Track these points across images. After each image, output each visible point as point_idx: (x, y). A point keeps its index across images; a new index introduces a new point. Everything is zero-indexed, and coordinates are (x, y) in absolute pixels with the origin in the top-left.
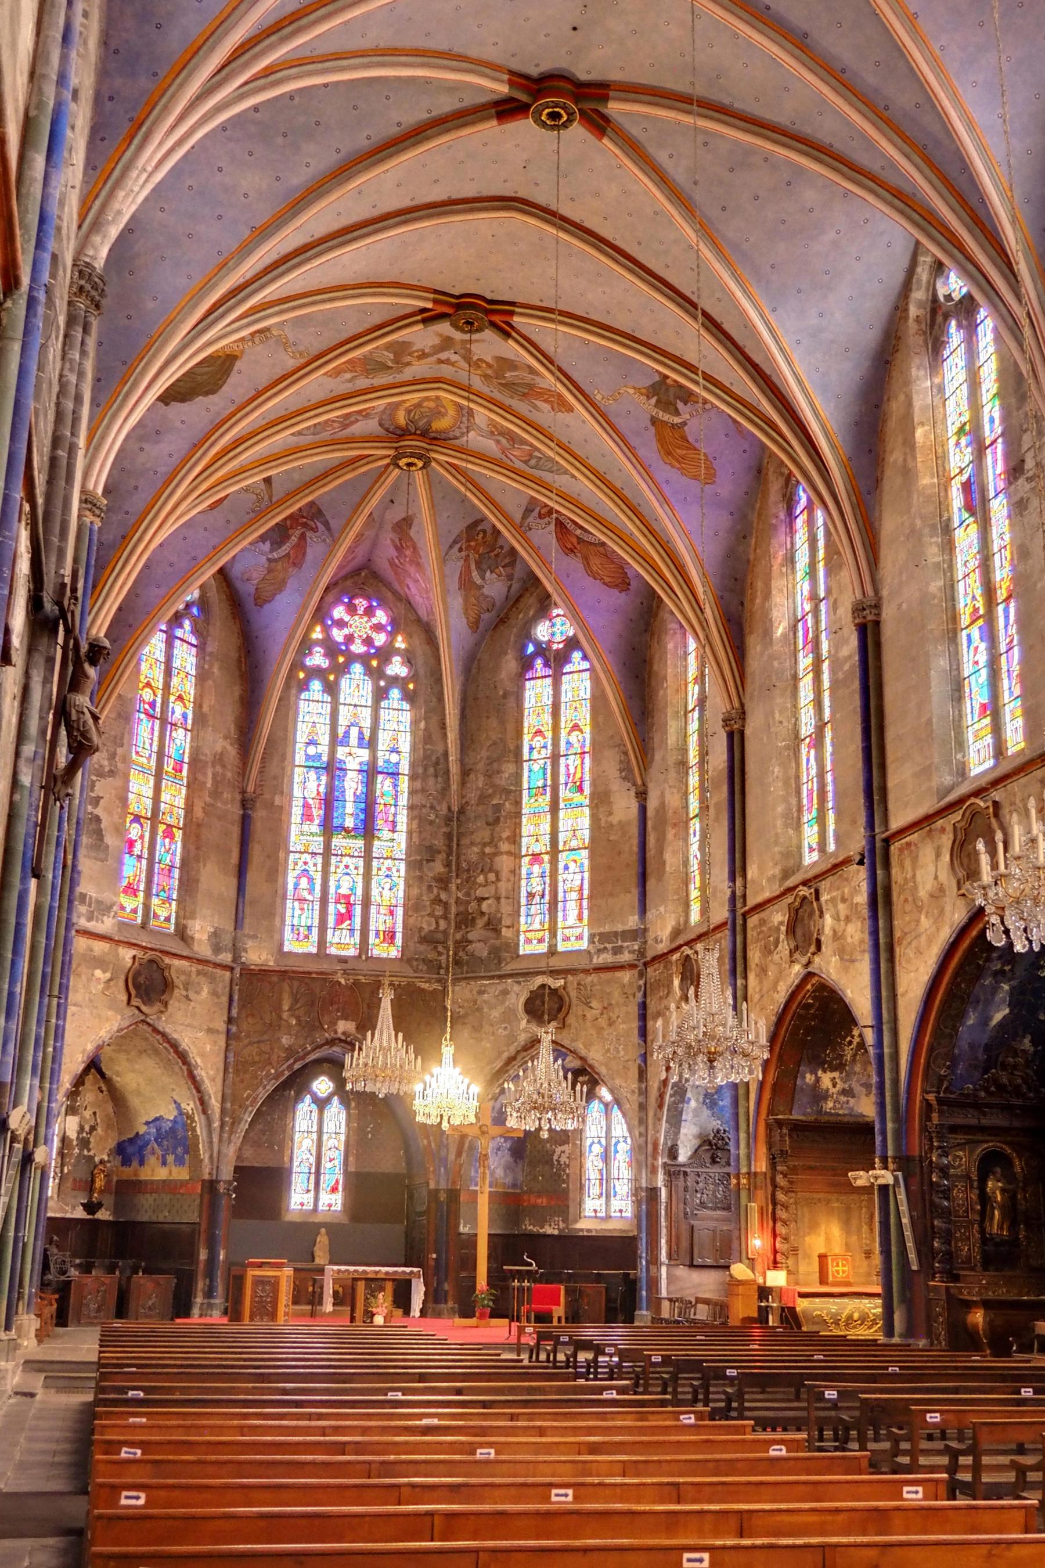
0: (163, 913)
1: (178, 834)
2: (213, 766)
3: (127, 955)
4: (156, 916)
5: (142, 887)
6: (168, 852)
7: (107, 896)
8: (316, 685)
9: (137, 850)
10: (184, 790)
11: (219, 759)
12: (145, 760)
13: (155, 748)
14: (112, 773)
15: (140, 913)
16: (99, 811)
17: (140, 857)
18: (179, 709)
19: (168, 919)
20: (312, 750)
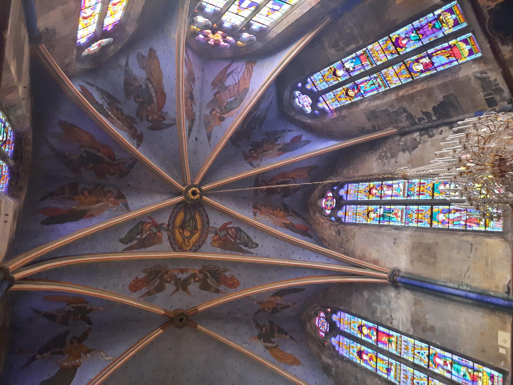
0: (450, 18)
1: (394, 36)
2: (343, 49)
3: (506, 50)
4: (456, 23)
5: (446, 45)
6: (409, 38)
7: (475, 85)
8: (255, 26)
9: (426, 60)
10: (369, 47)
11: (336, 46)
12: (379, 80)
13: (367, 78)
14: (405, 110)
15: (463, 37)
16: (430, 110)
17: (430, 56)
18: (340, 73)
19: (450, 11)
20: (276, 7)
